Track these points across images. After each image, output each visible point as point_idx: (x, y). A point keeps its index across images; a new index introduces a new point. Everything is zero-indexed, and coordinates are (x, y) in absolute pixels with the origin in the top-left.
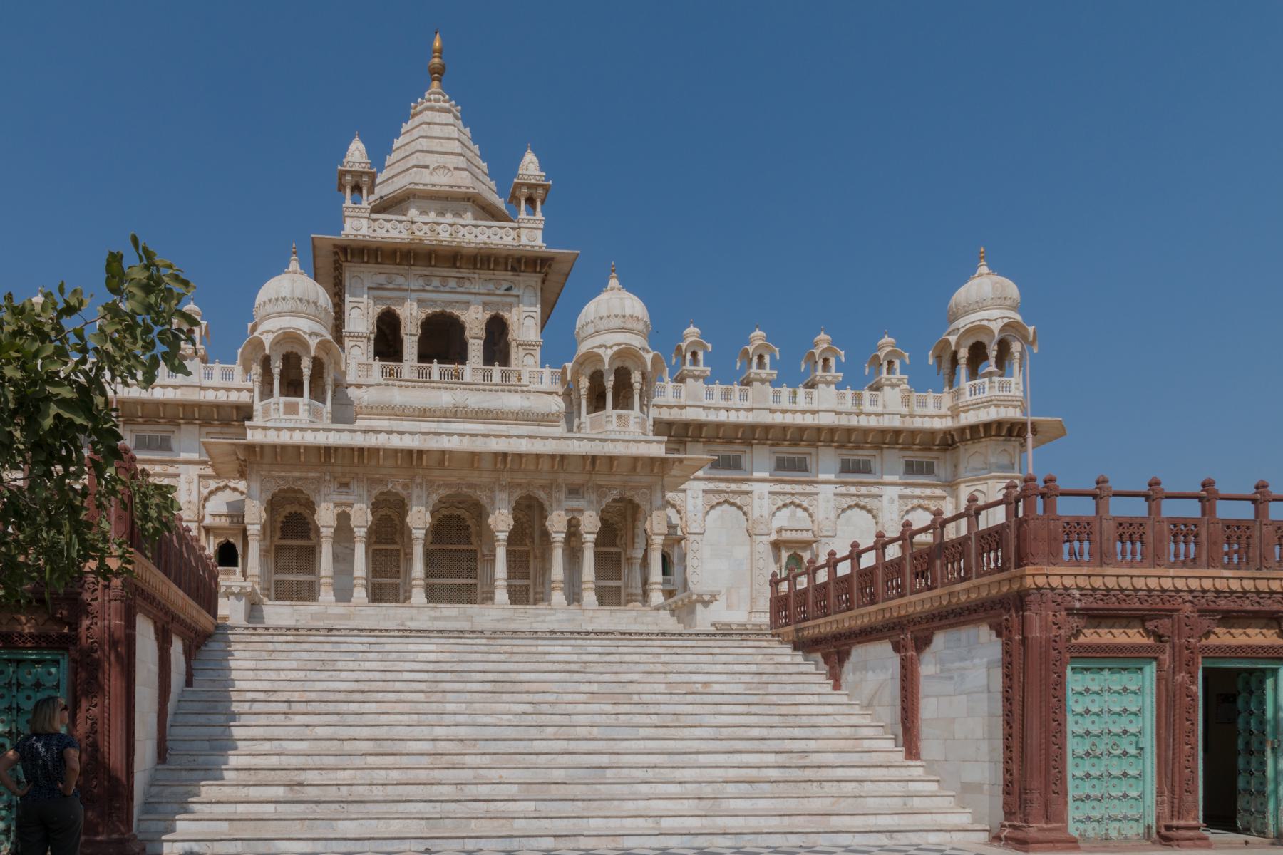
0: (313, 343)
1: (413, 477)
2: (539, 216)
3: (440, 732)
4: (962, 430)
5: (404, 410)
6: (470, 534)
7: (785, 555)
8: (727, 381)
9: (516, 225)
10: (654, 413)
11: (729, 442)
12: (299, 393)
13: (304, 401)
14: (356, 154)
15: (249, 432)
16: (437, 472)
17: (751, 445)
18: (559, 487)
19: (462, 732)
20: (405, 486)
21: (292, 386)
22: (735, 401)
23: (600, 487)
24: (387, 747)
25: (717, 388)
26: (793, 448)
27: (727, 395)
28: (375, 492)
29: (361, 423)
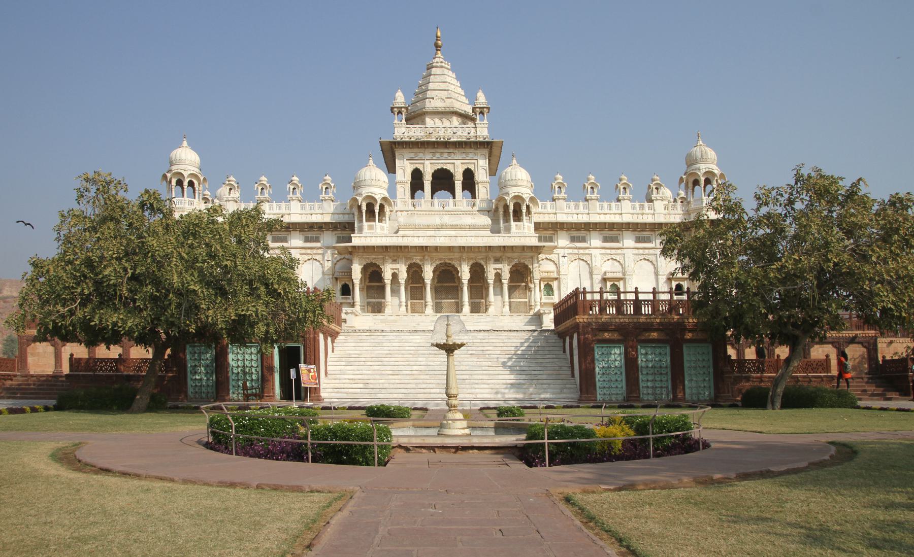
1: (424, 257)
3: (415, 368)
8: (576, 200)
12: (374, 221)
18: (490, 259)
19: (422, 368)
20: (421, 260)
24: (397, 372)
25: (572, 204)
26: (611, 231)
27: (577, 207)
28: (408, 263)
29: (400, 233)
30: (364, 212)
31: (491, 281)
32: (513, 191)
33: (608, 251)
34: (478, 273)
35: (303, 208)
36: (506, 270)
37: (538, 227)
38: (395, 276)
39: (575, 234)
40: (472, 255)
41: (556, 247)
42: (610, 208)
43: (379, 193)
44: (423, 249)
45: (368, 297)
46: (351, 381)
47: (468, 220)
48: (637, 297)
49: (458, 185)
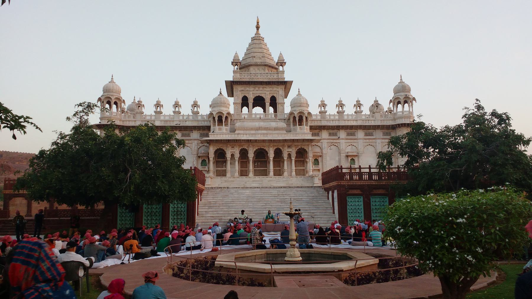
4: (396, 125)
7: (350, 159)
10: (309, 124)
13: (224, 127)
16: (255, 144)
20: (247, 147)
29: (236, 132)
30: (216, 121)
31: (285, 158)
33: (349, 141)
34: (278, 153)
36: (293, 152)
38: (233, 155)
39: (331, 131)
40: (275, 144)
41: (320, 140)
44: (248, 141)
46: (212, 218)
47: (274, 124)
48: (370, 170)
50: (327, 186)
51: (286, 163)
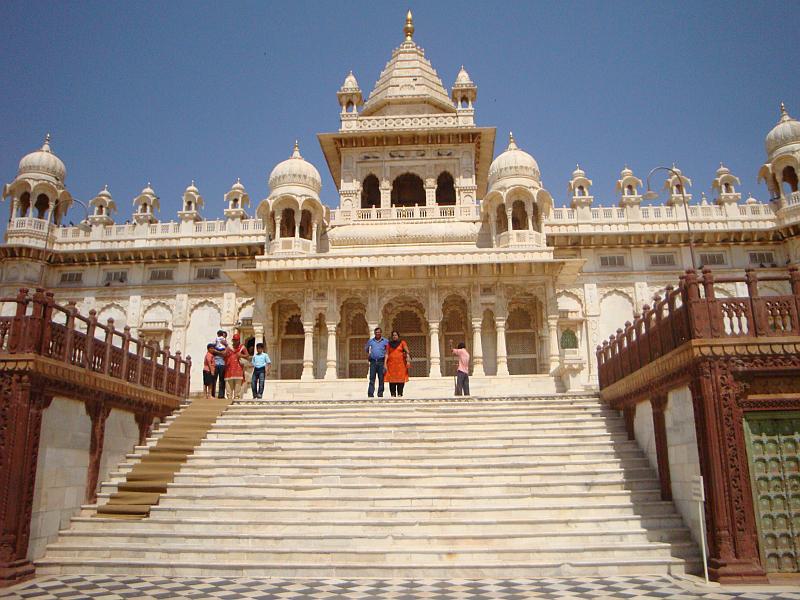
0: (301, 201)
2: (470, 107)
5: (371, 239)
6: (420, 325)
9: (454, 114)
10: (546, 230)
11: (611, 246)
14: (350, 83)
15: (258, 263)
16: (385, 282)
17: (630, 248)
18: (475, 287)
21: (288, 229)
22: (615, 218)
23: (507, 285)
25: (601, 210)
27: (608, 214)
28: (343, 299)
29: (332, 251)
31: (477, 324)
32: (511, 183)
35: (198, 229)
37: (551, 240)
39: (607, 253)
42: (658, 214)
43: (300, 194)
44: (367, 272)
45: (284, 357)
47: (441, 229)
49: (431, 195)
50: (621, 387)
51: (477, 337)
